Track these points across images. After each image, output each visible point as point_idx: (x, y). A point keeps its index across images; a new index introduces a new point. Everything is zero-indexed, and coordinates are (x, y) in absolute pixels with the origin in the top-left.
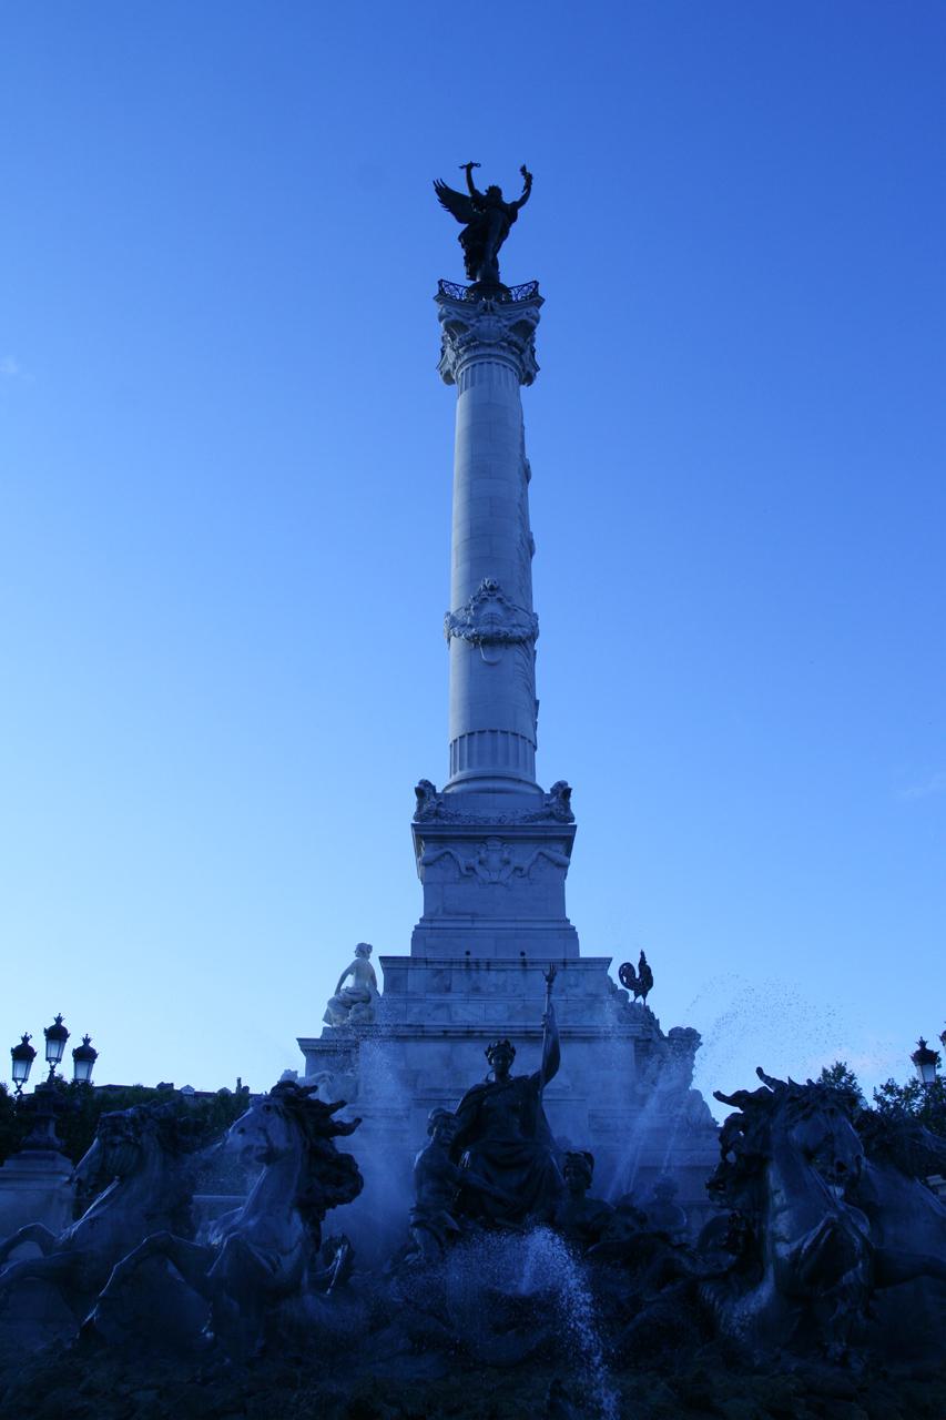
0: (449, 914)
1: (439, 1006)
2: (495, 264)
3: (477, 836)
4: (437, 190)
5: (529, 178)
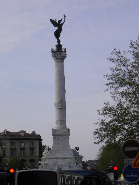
3: (59, 135)
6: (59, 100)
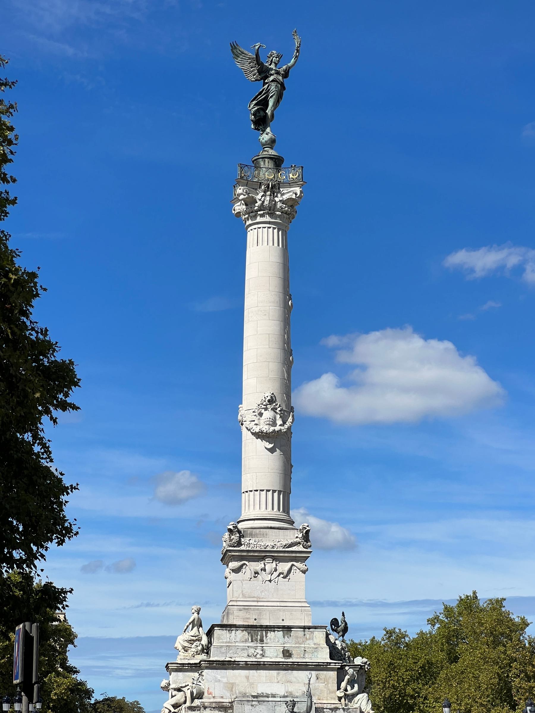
0: (245, 597)
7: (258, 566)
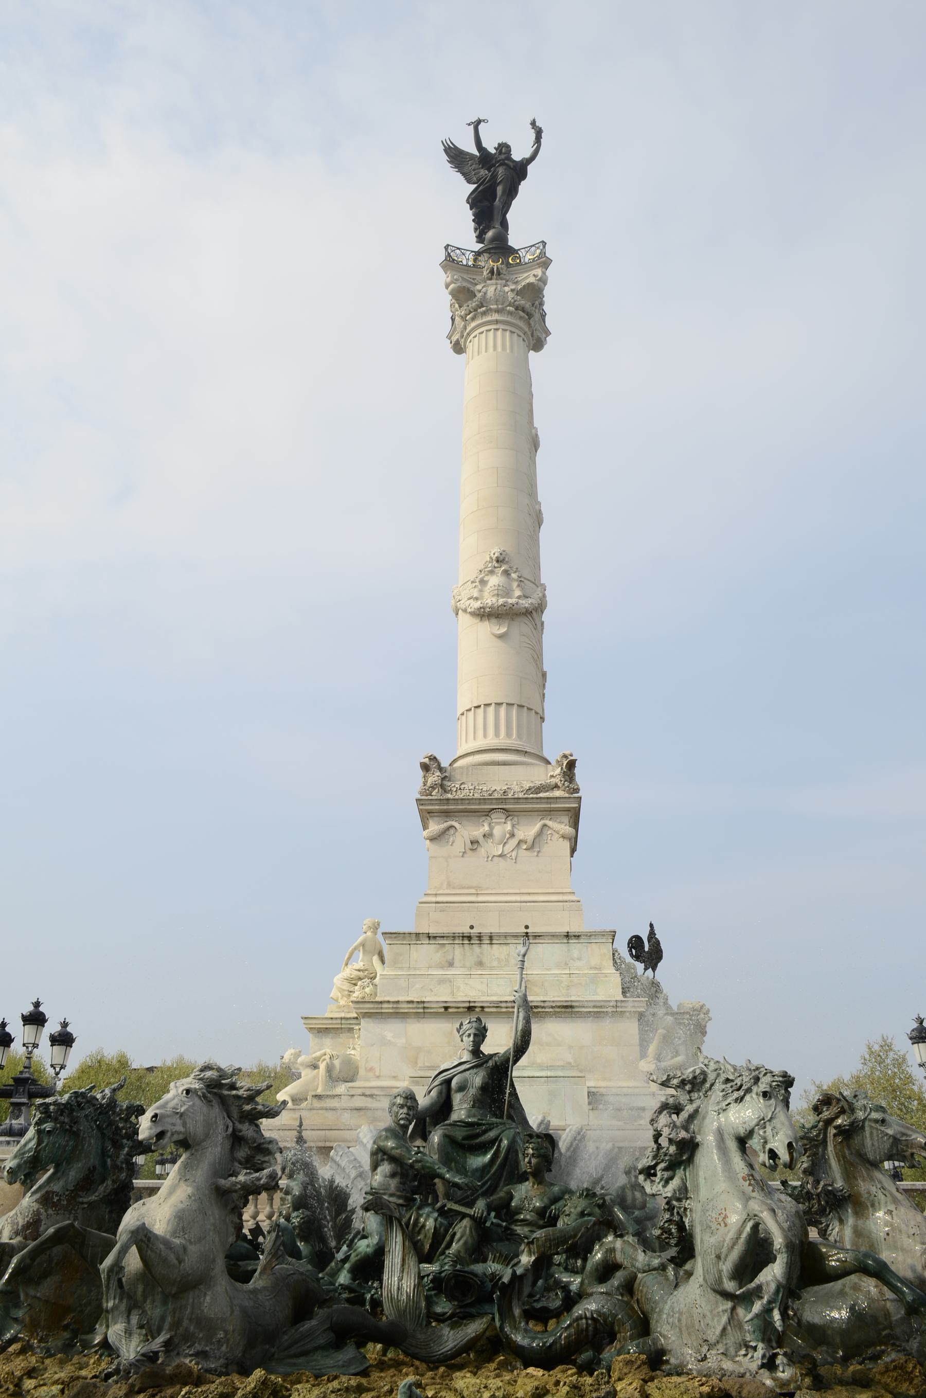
0: (454, 888)
1: (441, 981)
2: (504, 225)
4: (445, 150)
5: (539, 133)
6: (495, 551)
7: (477, 830)
